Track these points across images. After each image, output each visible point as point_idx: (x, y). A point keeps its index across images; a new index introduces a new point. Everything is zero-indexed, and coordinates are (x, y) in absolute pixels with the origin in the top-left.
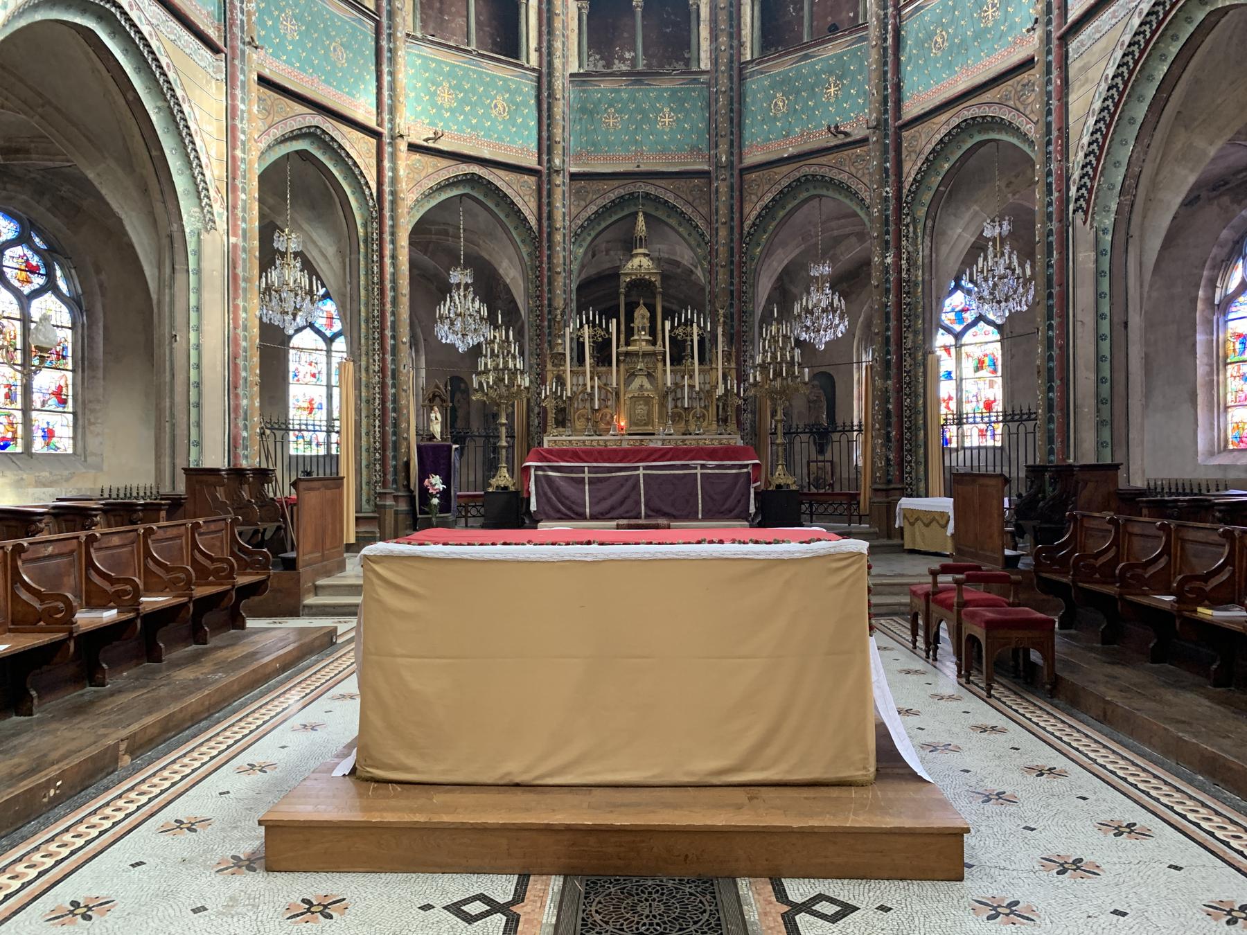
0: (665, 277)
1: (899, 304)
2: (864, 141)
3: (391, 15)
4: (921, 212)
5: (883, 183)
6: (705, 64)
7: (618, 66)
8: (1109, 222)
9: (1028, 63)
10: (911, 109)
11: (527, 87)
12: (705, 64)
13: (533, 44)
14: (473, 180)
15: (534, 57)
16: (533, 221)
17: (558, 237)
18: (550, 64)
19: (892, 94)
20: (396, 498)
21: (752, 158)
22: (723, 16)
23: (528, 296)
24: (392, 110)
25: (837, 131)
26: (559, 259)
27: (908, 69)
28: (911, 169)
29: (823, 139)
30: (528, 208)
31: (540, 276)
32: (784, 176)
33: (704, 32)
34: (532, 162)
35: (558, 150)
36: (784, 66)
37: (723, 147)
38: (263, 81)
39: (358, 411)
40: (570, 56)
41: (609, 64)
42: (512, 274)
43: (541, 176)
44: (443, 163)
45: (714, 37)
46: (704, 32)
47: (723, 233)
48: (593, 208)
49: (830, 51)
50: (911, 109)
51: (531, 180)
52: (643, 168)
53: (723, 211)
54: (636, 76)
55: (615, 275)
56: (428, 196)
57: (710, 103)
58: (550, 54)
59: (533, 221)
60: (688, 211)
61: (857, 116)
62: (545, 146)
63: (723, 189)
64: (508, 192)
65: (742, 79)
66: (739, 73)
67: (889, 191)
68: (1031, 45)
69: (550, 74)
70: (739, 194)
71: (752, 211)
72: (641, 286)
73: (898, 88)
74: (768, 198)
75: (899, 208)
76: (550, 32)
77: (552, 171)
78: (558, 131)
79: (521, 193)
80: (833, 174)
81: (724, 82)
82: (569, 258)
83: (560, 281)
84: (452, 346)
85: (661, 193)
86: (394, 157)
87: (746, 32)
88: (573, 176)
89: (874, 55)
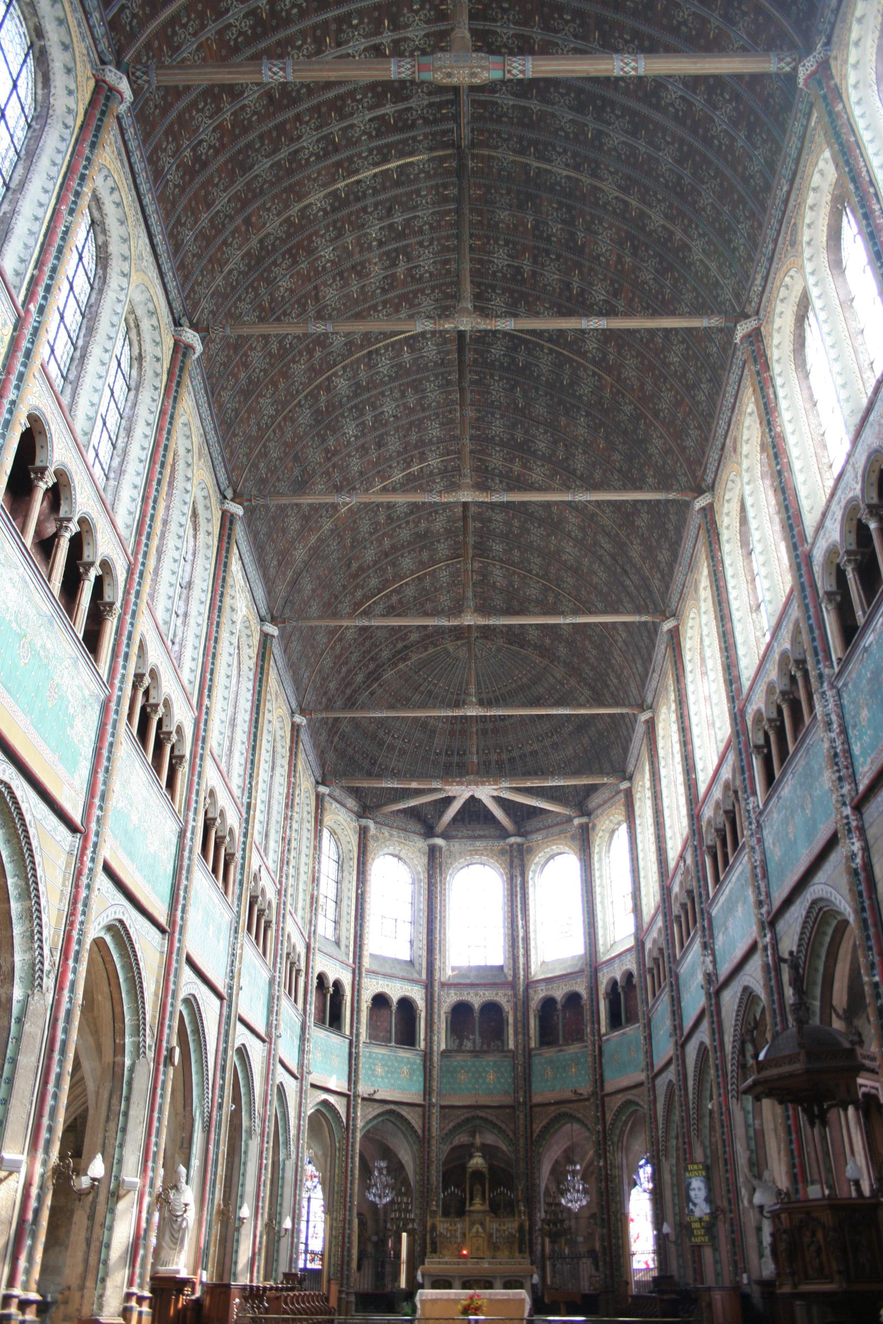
0: (491, 1167)
1: (607, 1187)
2: (588, 1099)
3: (358, 1036)
4: (615, 1139)
5: (597, 1124)
6: (511, 1046)
7: (468, 1045)
8: (674, 1161)
9: (641, 1084)
10: (609, 1088)
11: (419, 1061)
12: (511, 1046)
13: (422, 1037)
14: (391, 1112)
15: (423, 1044)
16: (420, 1132)
17: (434, 1142)
18: (431, 1048)
19: (599, 1080)
20: (348, 1294)
21: (537, 1099)
22: (520, 1025)
23: (415, 1173)
24: (356, 1083)
25: (575, 1092)
26: (433, 1155)
27: (606, 1068)
28: (609, 1117)
29: (568, 1095)
30: (416, 1121)
31: (424, 1164)
32: (553, 1111)
33: (511, 1031)
34: (419, 1100)
35: (435, 1094)
36: (549, 1053)
37: (521, 1093)
38: (313, 1086)
39: (330, 1243)
40: (441, 1042)
41: (461, 1044)
42: (406, 1155)
43: (424, 1108)
44: (376, 1105)
45: (516, 1034)
46: (511, 1031)
47: (522, 1141)
48: (452, 1125)
49: (573, 1049)
50: (609, 1088)
51: (419, 1110)
52: (480, 1103)
53: (522, 1129)
54: (476, 1053)
55: (463, 1167)
56: (367, 1123)
57: (514, 1068)
58: (431, 1042)
59: (420, 1132)
60: (504, 1126)
61: (585, 1087)
62: (427, 1091)
63: (522, 1116)
64: (408, 1117)
65: (530, 1056)
66: (528, 1054)
67: (599, 1127)
68: (642, 1077)
69: (431, 1053)
70: (530, 1119)
71: (537, 1128)
72: (477, 1174)
73: (601, 1075)
74: (544, 1123)
75: (605, 1138)
76: (432, 1031)
77: (431, 1105)
78: (435, 1084)
79: (414, 1118)
80: (575, 1113)
81: (521, 1059)
82: (439, 1152)
83: (434, 1167)
84: (374, 1204)
85: (490, 1118)
86: (355, 1107)
87: (532, 1032)
88: (442, 1107)
89: (590, 1059)
